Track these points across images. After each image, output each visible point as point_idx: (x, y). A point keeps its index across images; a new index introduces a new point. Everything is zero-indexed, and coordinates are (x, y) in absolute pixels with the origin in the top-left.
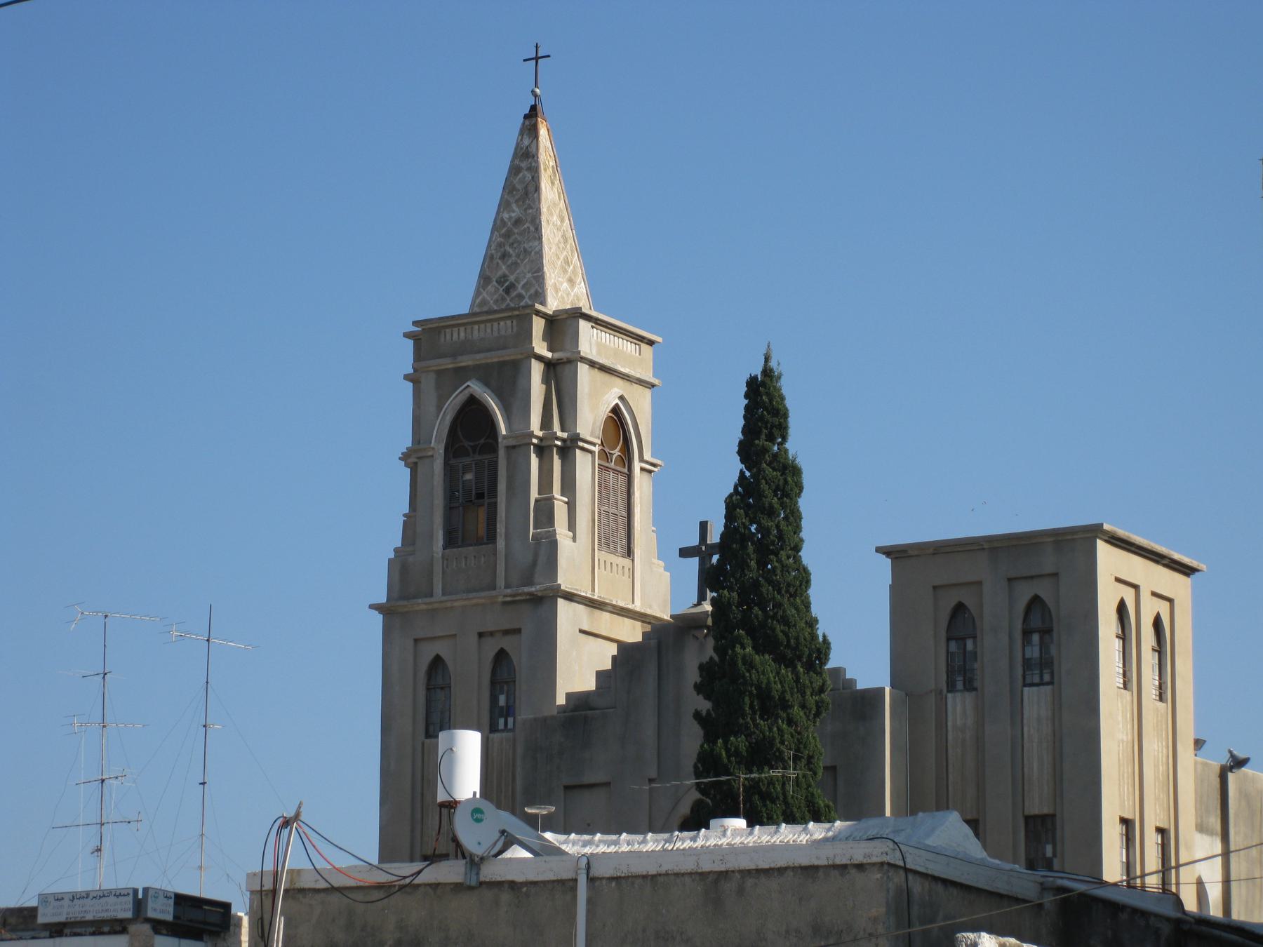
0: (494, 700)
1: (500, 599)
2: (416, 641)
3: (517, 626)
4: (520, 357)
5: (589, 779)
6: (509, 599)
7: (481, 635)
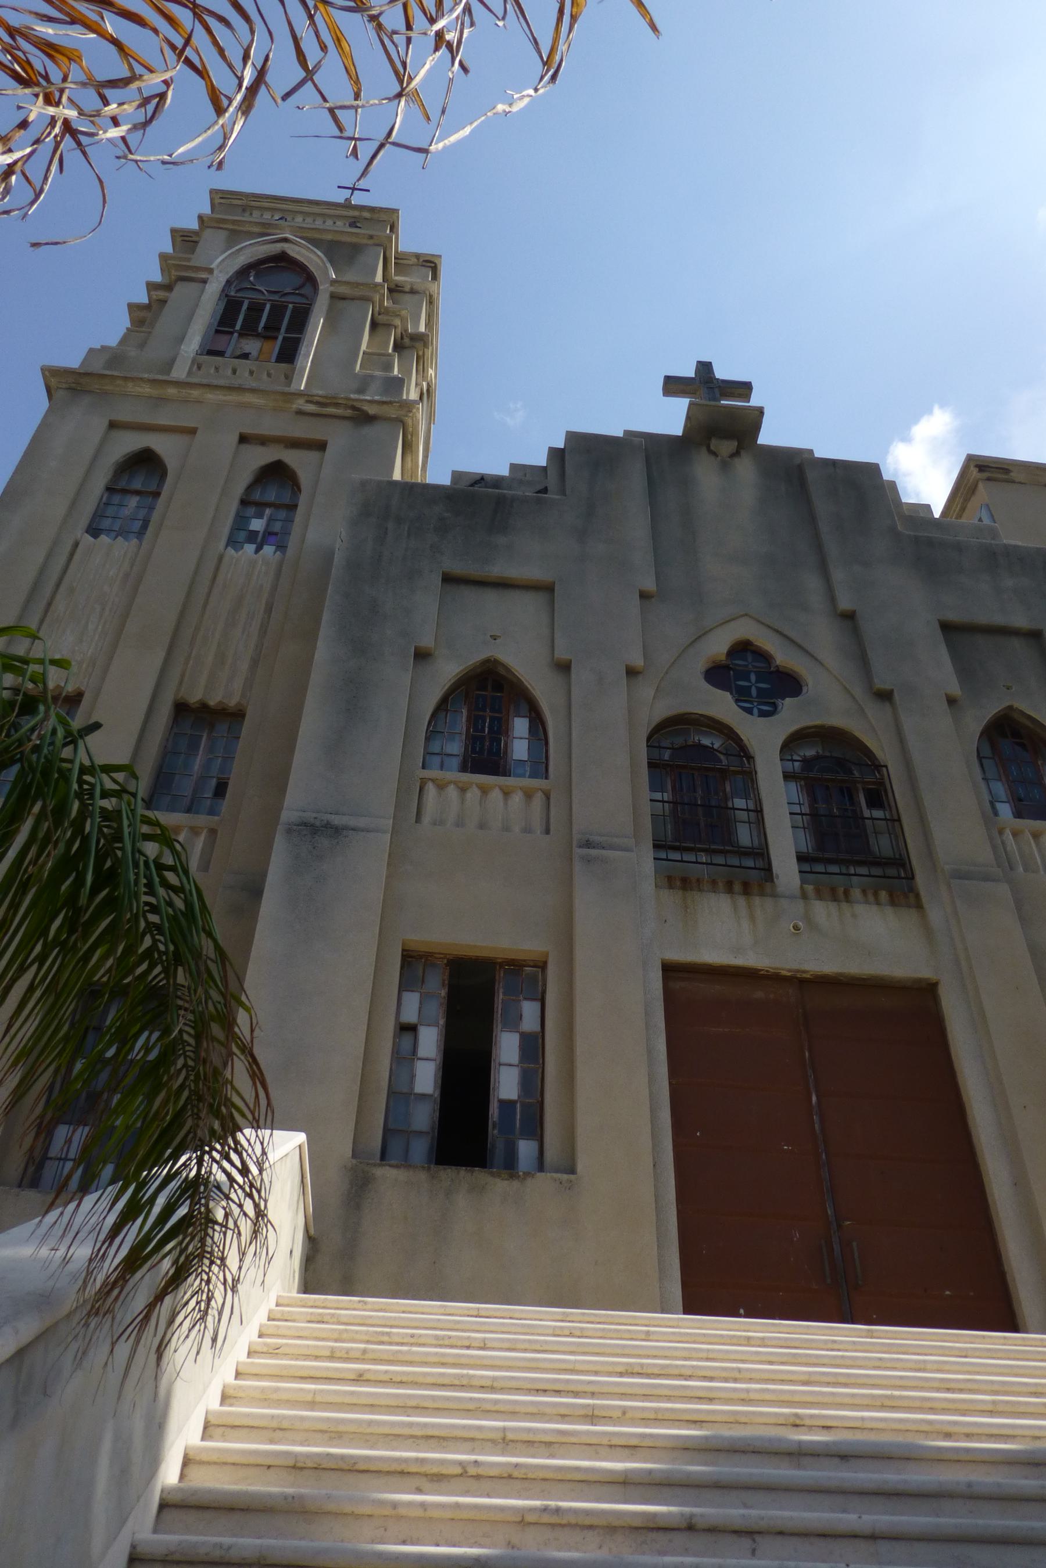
0: (240, 522)
1: (300, 404)
2: (113, 425)
3: (317, 436)
4: (365, 241)
5: (498, 570)
6: (311, 408)
7: (243, 439)
